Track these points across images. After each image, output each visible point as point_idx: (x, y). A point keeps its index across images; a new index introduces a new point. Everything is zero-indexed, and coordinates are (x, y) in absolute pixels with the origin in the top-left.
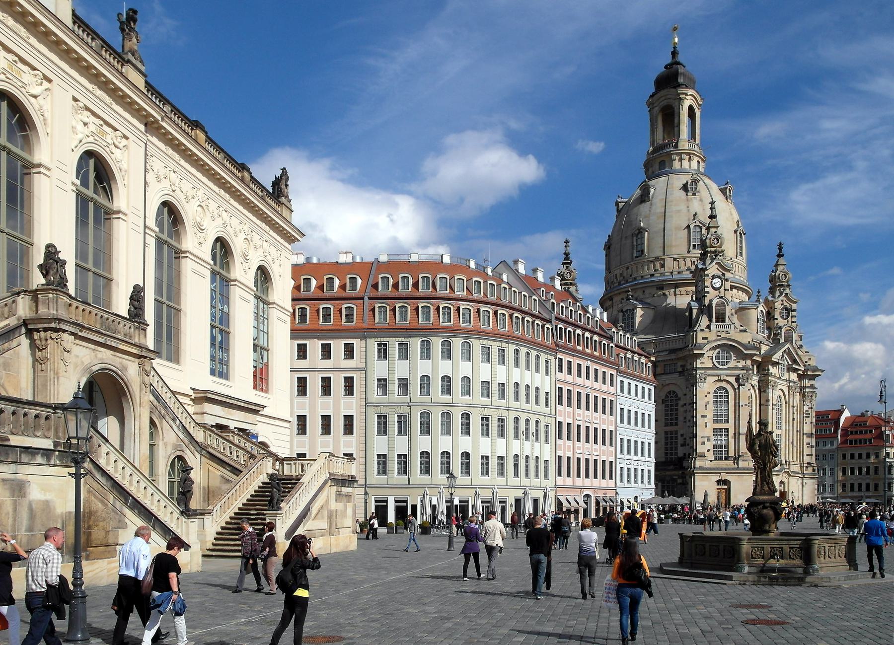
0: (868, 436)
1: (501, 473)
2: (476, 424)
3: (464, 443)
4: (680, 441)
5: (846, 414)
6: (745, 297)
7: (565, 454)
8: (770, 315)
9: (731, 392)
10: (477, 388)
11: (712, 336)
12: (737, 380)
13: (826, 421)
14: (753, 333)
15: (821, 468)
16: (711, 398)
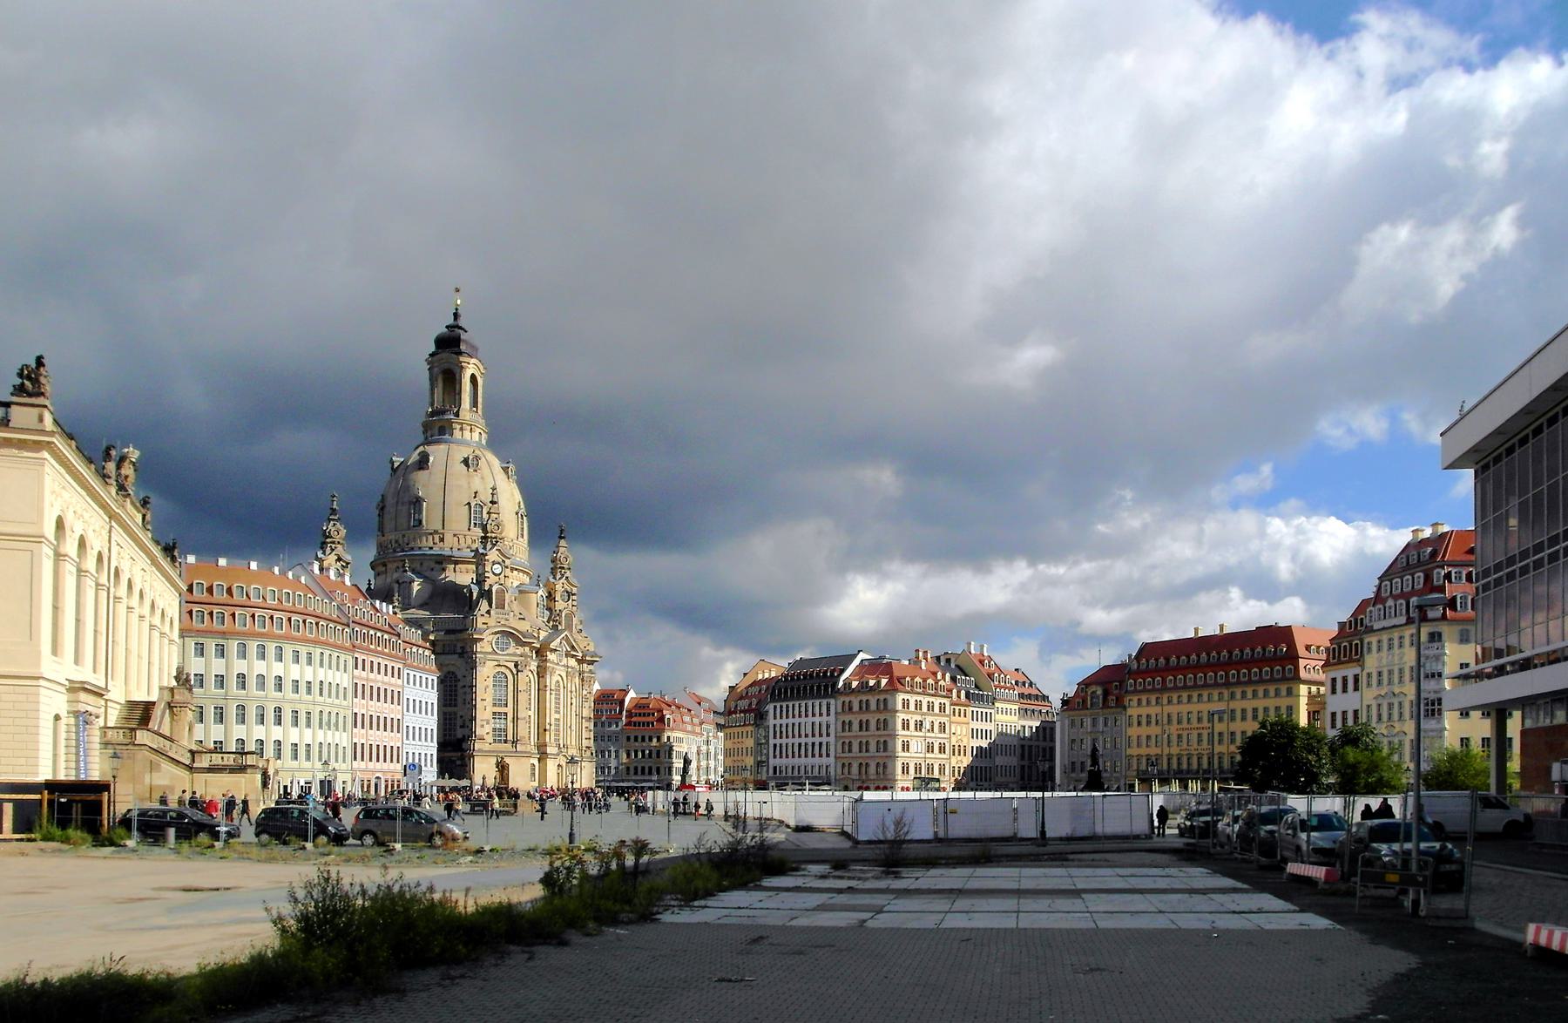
0: (650, 719)
1: (308, 758)
2: (287, 716)
3: (277, 733)
4: (459, 722)
5: (632, 694)
6: (526, 579)
7: (359, 741)
8: (551, 597)
9: (510, 677)
10: (287, 686)
11: (492, 622)
12: (516, 666)
13: (607, 702)
14: (532, 620)
15: (601, 752)
16: (490, 682)
